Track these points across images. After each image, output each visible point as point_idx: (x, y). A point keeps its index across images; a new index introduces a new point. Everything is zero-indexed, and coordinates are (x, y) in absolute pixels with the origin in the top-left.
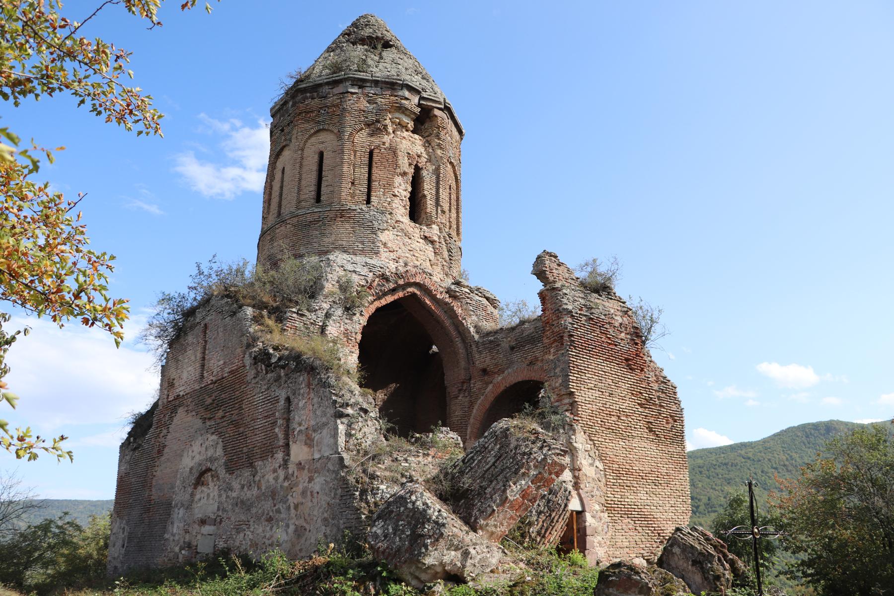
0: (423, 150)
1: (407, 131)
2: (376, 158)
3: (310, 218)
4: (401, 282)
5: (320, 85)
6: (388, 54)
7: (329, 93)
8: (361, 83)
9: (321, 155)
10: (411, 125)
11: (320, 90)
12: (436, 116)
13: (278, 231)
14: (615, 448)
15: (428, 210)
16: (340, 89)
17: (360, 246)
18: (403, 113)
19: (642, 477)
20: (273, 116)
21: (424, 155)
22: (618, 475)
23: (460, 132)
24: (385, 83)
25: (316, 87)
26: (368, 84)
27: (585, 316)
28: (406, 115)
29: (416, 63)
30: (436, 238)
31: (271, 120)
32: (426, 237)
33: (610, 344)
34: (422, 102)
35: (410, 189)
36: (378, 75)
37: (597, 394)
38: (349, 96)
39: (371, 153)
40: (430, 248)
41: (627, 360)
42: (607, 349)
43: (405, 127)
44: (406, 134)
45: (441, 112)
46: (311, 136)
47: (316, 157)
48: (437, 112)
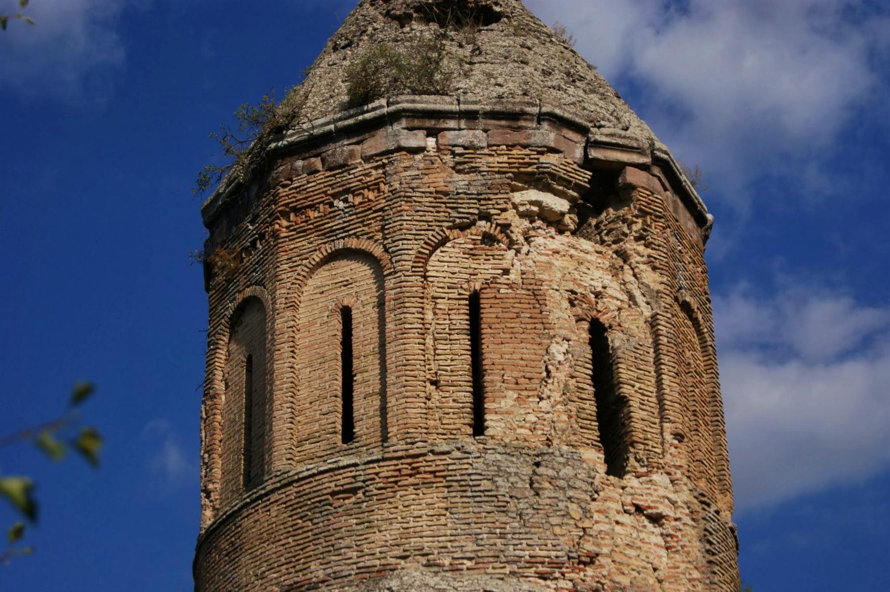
0: (608, 279)
1: (561, 232)
2: (488, 314)
3: (329, 484)
5: (328, 138)
6: (493, 38)
7: (352, 155)
8: (431, 121)
9: (346, 313)
11: (330, 148)
12: (633, 187)
13: (246, 523)
15: (638, 436)
17: (471, 546)
18: (547, 188)
20: (209, 225)
21: (614, 289)
23: (700, 220)
24: (493, 115)
25: (314, 144)
26: (452, 124)
28: (556, 193)
29: (568, 54)
30: (664, 509)
31: (206, 233)
32: (639, 509)
34: (594, 154)
36: (470, 97)
38: (402, 160)
39: (474, 302)
40: (652, 535)
43: (554, 221)
45: (644, 174)
46: (313, 270)
47: (337, 324)
48: (633, 176)
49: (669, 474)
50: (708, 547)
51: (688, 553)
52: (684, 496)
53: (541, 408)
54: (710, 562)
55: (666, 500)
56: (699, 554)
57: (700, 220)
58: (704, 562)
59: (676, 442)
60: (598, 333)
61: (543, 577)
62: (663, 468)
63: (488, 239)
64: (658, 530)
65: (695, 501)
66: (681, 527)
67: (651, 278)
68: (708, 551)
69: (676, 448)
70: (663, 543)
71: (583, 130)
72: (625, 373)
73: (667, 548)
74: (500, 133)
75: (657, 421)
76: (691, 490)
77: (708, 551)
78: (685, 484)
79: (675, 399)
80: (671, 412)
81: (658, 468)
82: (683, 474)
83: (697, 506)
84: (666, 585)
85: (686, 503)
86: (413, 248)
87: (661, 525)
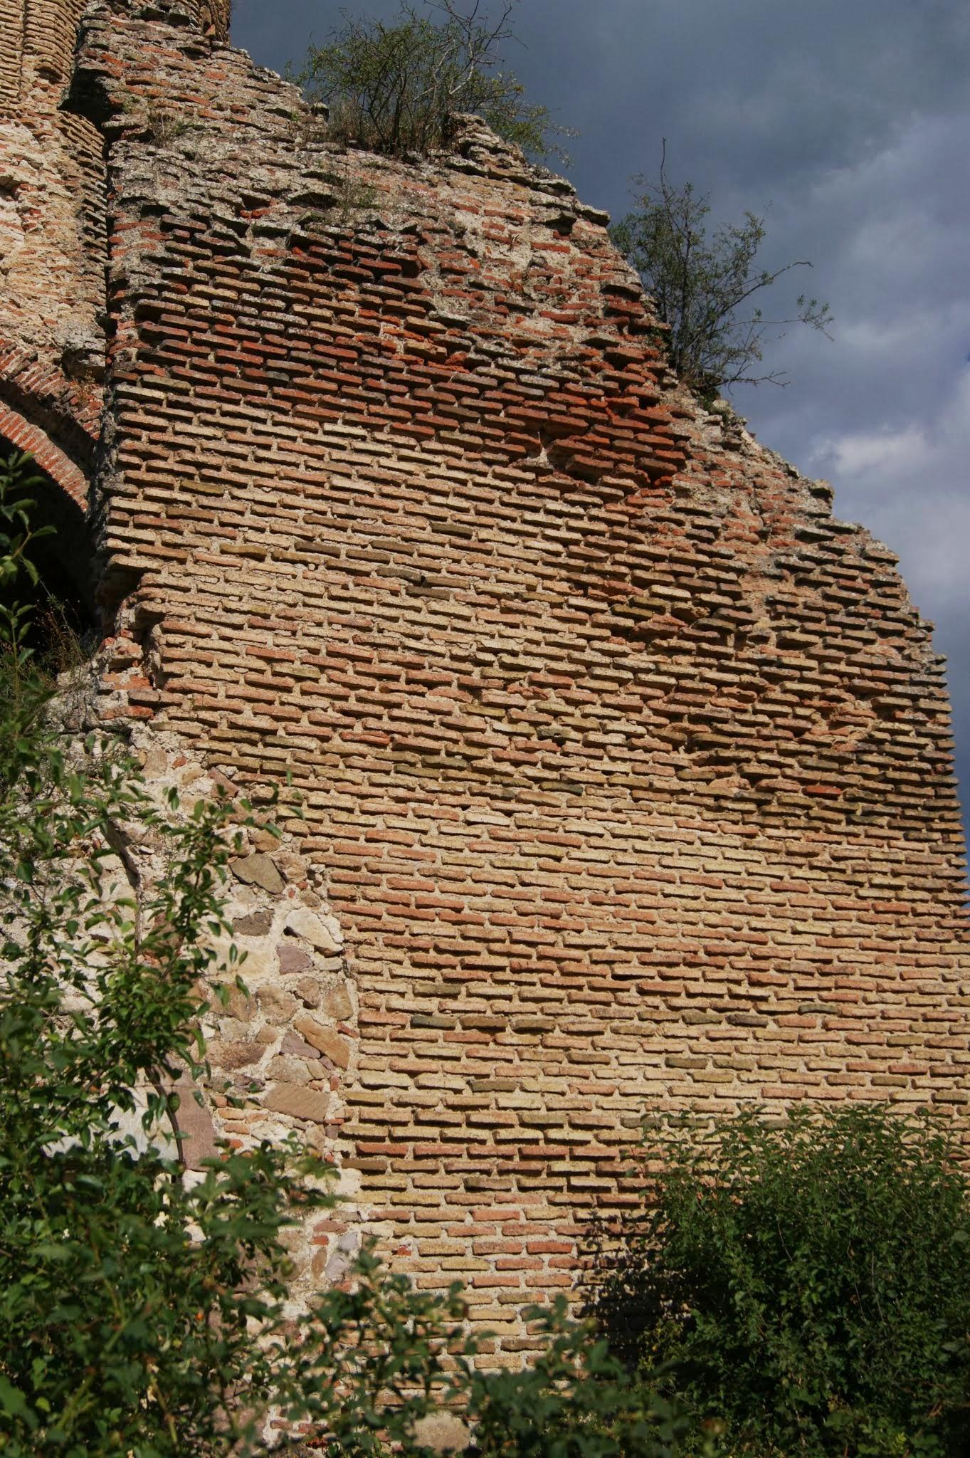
14: (456, 847)
22: (452, 969)
27: (271, 233)
30: (20, 175)
33: (426, 356)
41: (549, 432)
49: (29, 125)
50: (90, 224)
51: (51, 232)
52: (54, 153)
54: (88, 244)
55: (24, 163)
56: (69, 234)
58: (79, 244)
59: (46, 82)
62: (19, 116)
64: (13, 204)
65: (73, 162)
66: (46, 197)
68: (86, 230)
69: (45, 89)
70: (19, 222)
73: (25, 228)
75: (18, 54)
76: (64, 147)
77: (86, 230)
78: (57, 140)
79: (45, 23)
80: (37, 40)
81: (10, 116)
82: (54, 125)
83: (73, 167)
84: (12, 276)
85: (55, 165)
87: (16, 199)
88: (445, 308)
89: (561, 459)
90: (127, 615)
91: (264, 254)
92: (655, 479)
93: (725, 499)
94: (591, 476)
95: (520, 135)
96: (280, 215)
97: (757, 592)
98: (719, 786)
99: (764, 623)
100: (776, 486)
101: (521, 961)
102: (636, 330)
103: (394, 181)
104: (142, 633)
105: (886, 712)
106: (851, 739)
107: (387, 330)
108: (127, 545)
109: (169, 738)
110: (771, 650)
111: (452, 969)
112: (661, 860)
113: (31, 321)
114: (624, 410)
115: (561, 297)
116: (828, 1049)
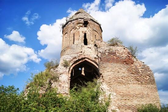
4: (80, 58)
10: (83, 26)
14: (123, 88)
16: (68, 24)
18: (80, 24)
19: (136, 96)
21: (87, 31)
24: (76, 19)
35: (84, 38)
37: (112, 73)
40: (90, 49)
41: (125, 62)
42: (118, 60)
43: (82, 26)
44: (82, 28)
48: (88, 21)
53: (79, 41)
57: (98, 24)
60: (85, 34)
61: (77, 54)
63: (75, 29)
67: (90, 29)
71: (83, 19)
72: (87, 37)
74: (76, 20)
86: (69, 31)
88: (118, 55)
89: (126, 63)
90: (101, 76)
91: (107, 54)
92: (132, 63)
93: (137, 64)
94: (128, 64)
95: (121, 43)
96: (107, 51)
97: (140, 70)
98: (139, 83)
99: (140, 72)
100: (140, 63)
101: (127, 95)
102: (130, 54)
103: (114, 48)
104: (102, 77)
105: (150, 77)
106: (147, 79)
107: (114, 57)
108: (101, 72)
109: (104, 83)
110: (141, 73)
111: (123, 96)
112: (135, 88)
113: (92, 56)
114: (130, 59)
115: (125, 53)
116: (148, 99)
